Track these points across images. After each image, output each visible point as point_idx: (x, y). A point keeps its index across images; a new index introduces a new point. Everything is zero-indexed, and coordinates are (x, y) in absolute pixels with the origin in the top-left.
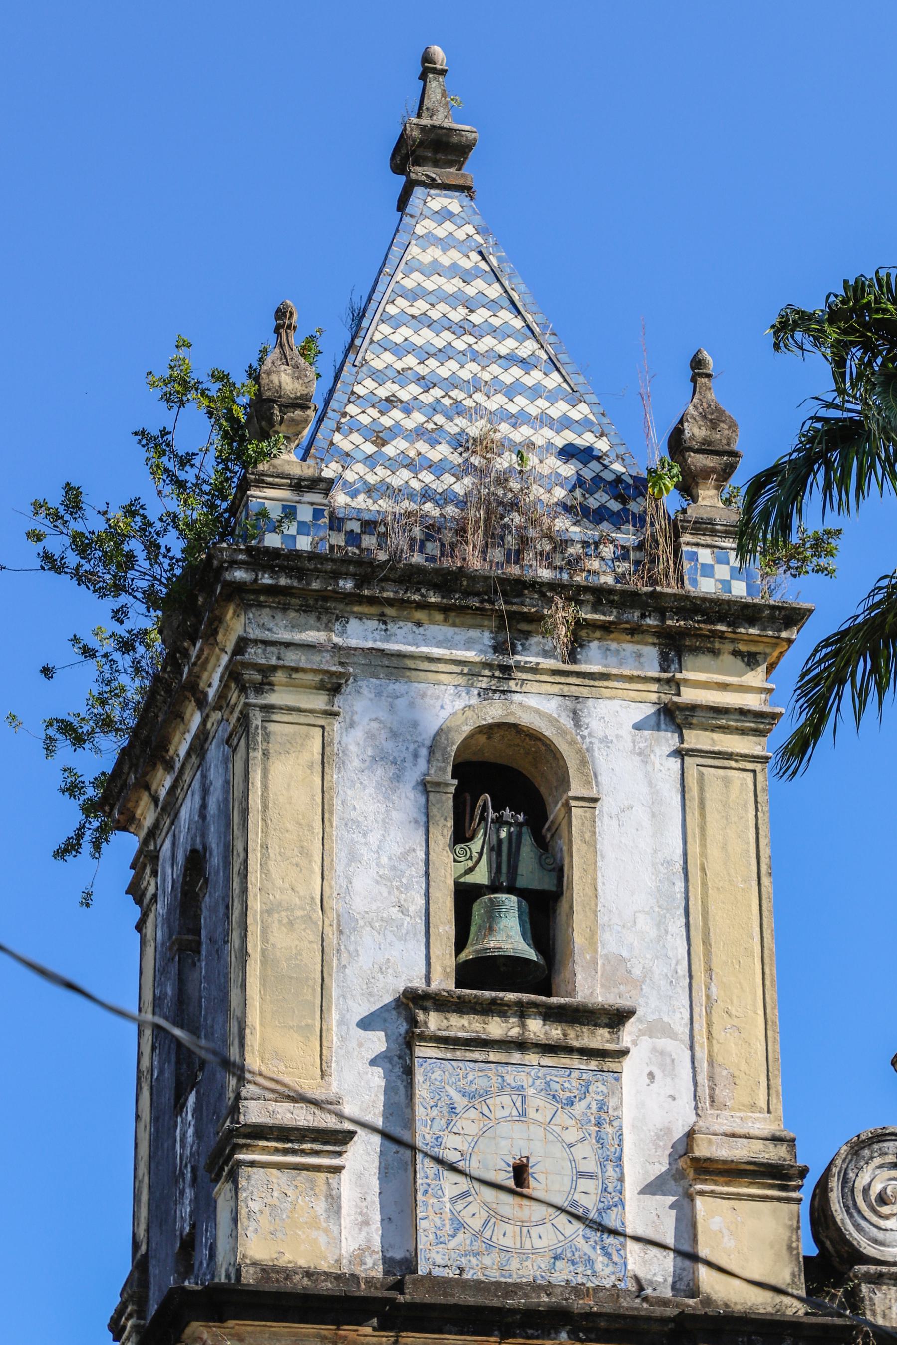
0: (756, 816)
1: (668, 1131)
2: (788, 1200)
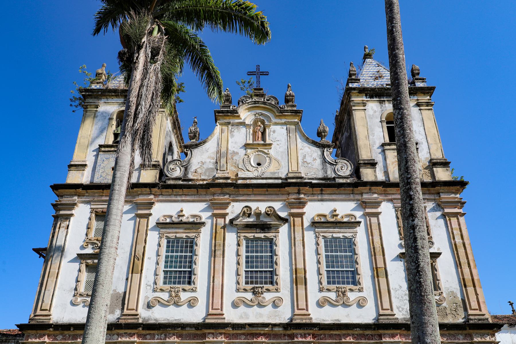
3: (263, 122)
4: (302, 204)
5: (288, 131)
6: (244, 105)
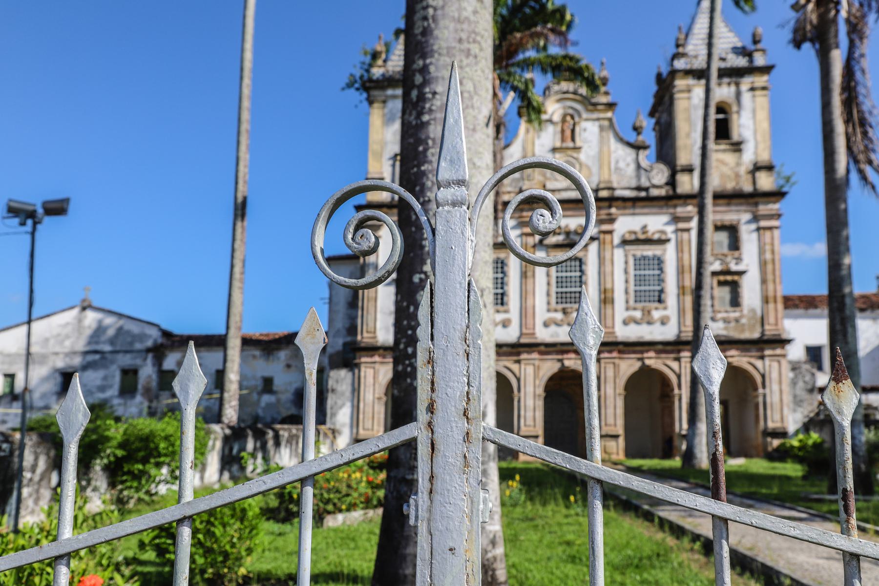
3: (572, 117)
4: (611, 220)
5: (602, 128)
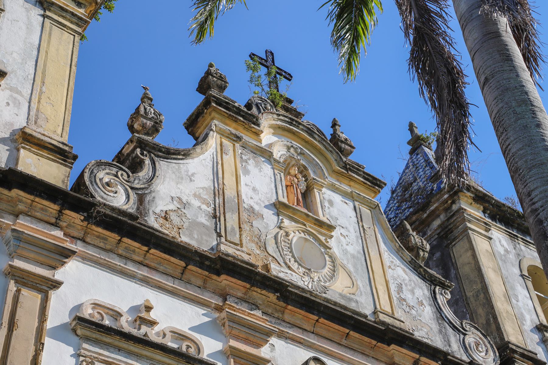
0: (73, 48)
1: (12, 124)
2: (66, 166)
3: (303, 171)
6: (270, 116)
